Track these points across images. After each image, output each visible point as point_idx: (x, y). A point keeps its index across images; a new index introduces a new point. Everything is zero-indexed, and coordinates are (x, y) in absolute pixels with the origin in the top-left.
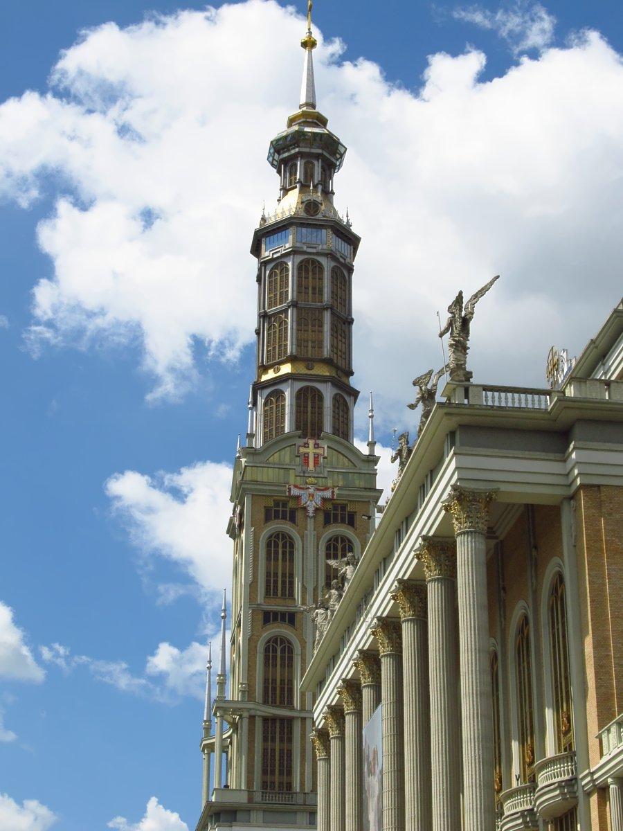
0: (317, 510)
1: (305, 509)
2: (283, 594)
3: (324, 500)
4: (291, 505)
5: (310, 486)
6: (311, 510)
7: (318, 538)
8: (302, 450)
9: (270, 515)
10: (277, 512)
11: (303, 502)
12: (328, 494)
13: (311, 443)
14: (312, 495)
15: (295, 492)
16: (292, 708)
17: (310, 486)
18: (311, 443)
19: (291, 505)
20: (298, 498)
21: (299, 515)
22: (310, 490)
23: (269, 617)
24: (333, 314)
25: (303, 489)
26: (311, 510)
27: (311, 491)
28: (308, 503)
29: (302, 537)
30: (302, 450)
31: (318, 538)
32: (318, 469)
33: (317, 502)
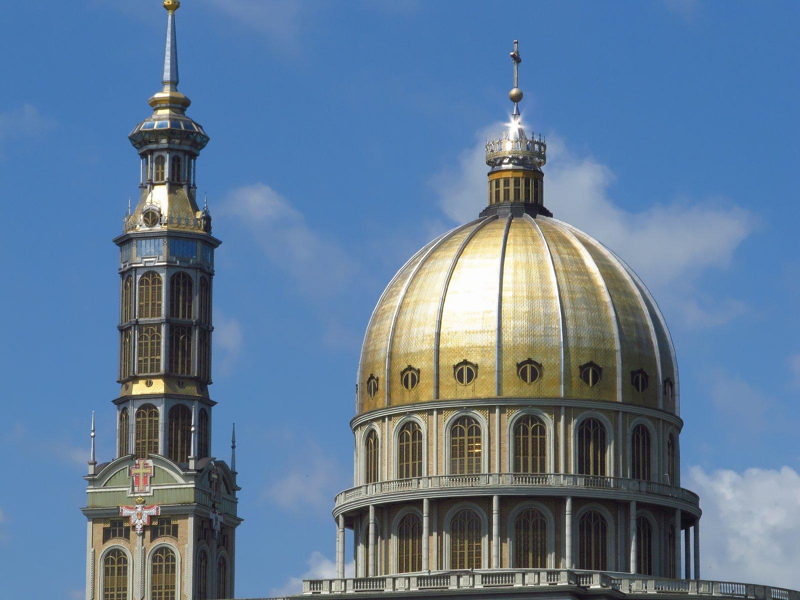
0: (145, 528)
1: (134, 527)
3: (151, 518)
4: (126, 525)
5: (138, 506)
6: (139, 527)
8: (134, 471)
11: (133, 521)
12: (153, 512)
14: (140, 515)
15: (126, 512)
17: (138, 506)
19: (126, 525)
20: (127, 518)
21: (132, 532)
22: (138, 509)
25: (132, 508)
27: (139, 510)
28: (137, 522)
29: (132, 554)
33: (145, 520)
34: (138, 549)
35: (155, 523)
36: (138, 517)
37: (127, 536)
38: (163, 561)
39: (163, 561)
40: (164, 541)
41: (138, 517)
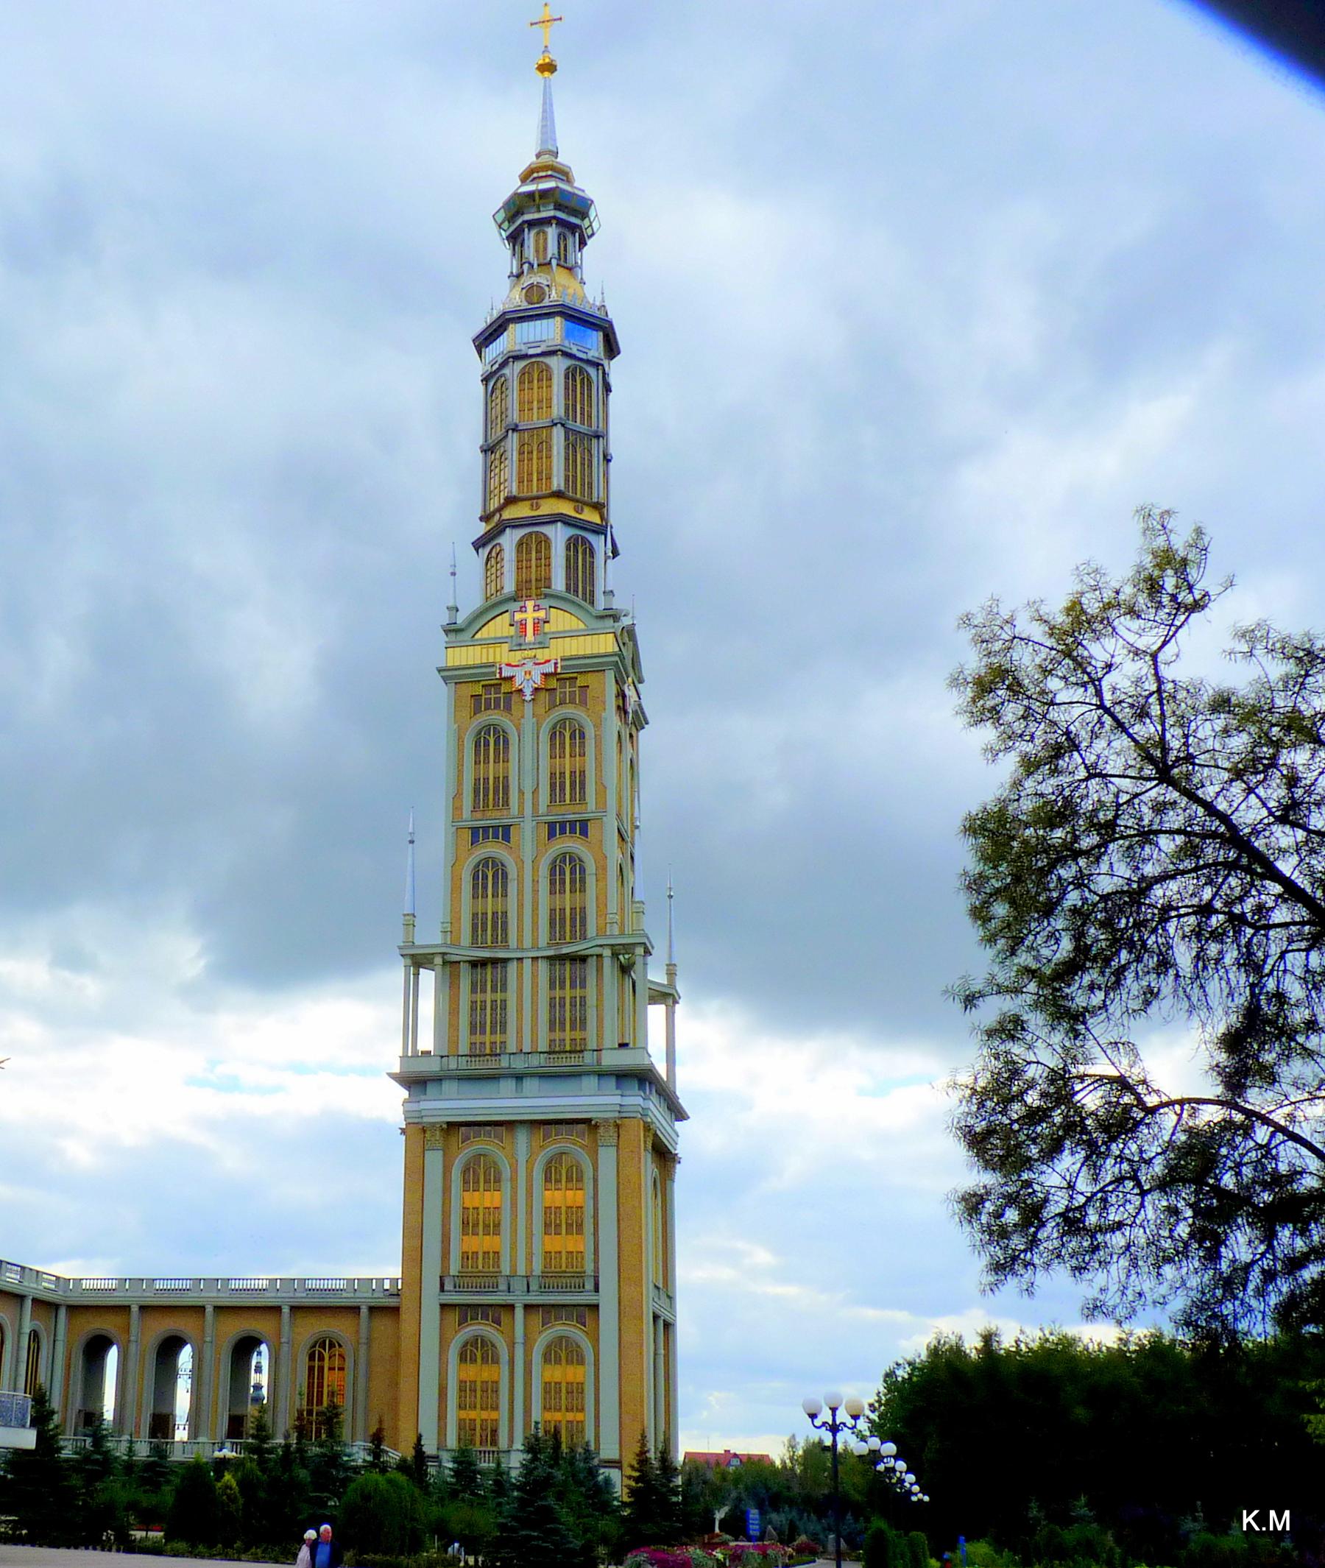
2: (496, 804)
3: (546, 675)
4: (505, 688)
6: (528, 691)
7: (539, 725)
8: (518, 616)
9: (478, 704)
10: (488, 701)
13: (530, 604)
16: (507, 947)
18: (530, 604)
20: (510, 679)
21: (515, 698)
23: (478, 834)
24: (567, 430)
26: (528, 691)
29: (518, 730)
30: (518, 616)
31: (539, 725)
32: (539, 638)
33: (538, 680)
34: (528, 723)
35: (553, 683)
36: (527, 678)
37: (508, 708)
38: (567, 737)
39: (567, 737)
40: (568, 710)
41: (527, 678)
